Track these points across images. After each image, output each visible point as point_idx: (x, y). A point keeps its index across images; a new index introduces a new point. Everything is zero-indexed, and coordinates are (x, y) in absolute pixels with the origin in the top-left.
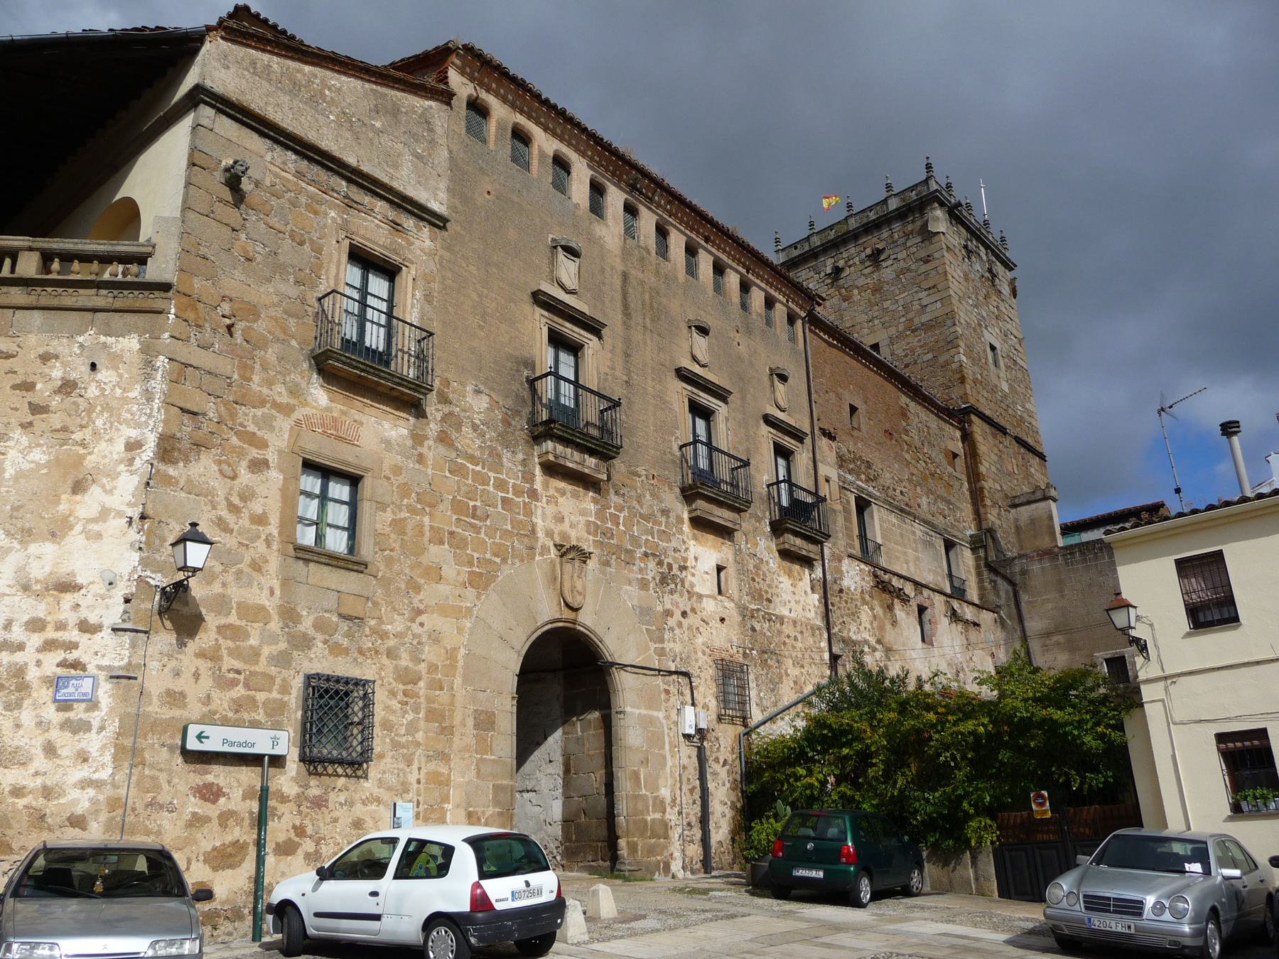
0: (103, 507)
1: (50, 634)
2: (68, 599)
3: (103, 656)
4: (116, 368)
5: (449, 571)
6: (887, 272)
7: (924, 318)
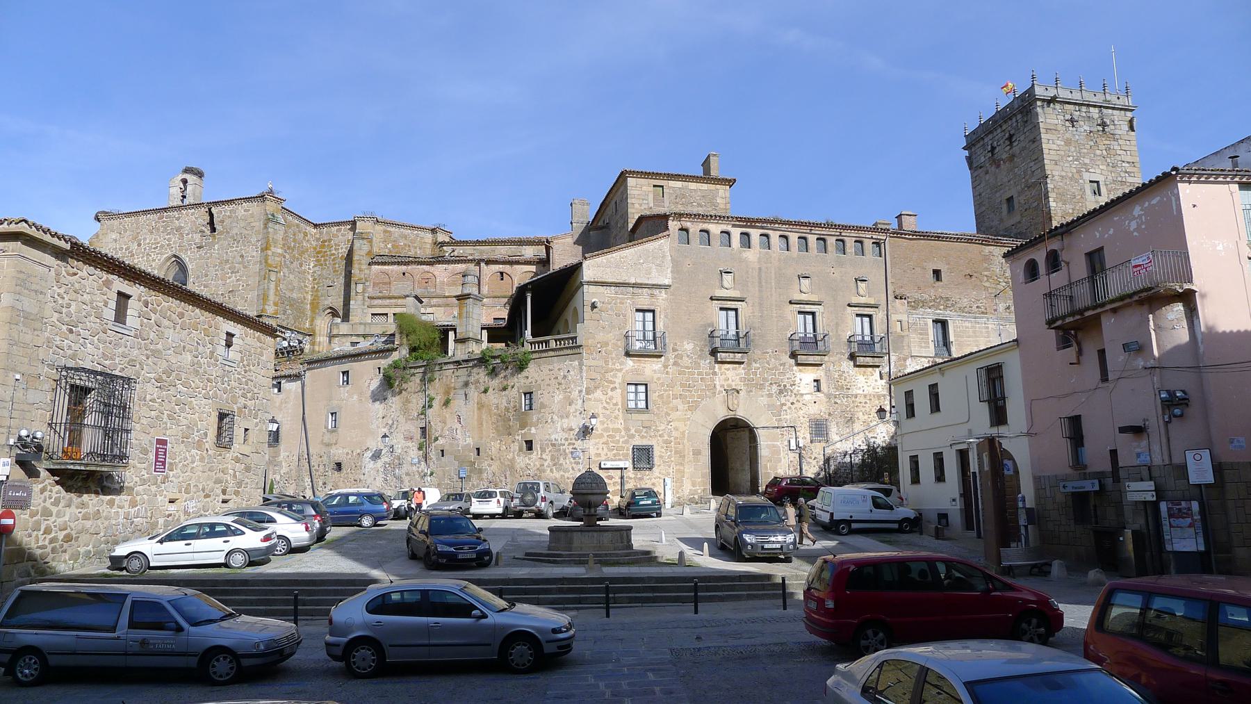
5: (680, 407)
6: (1016, 149)
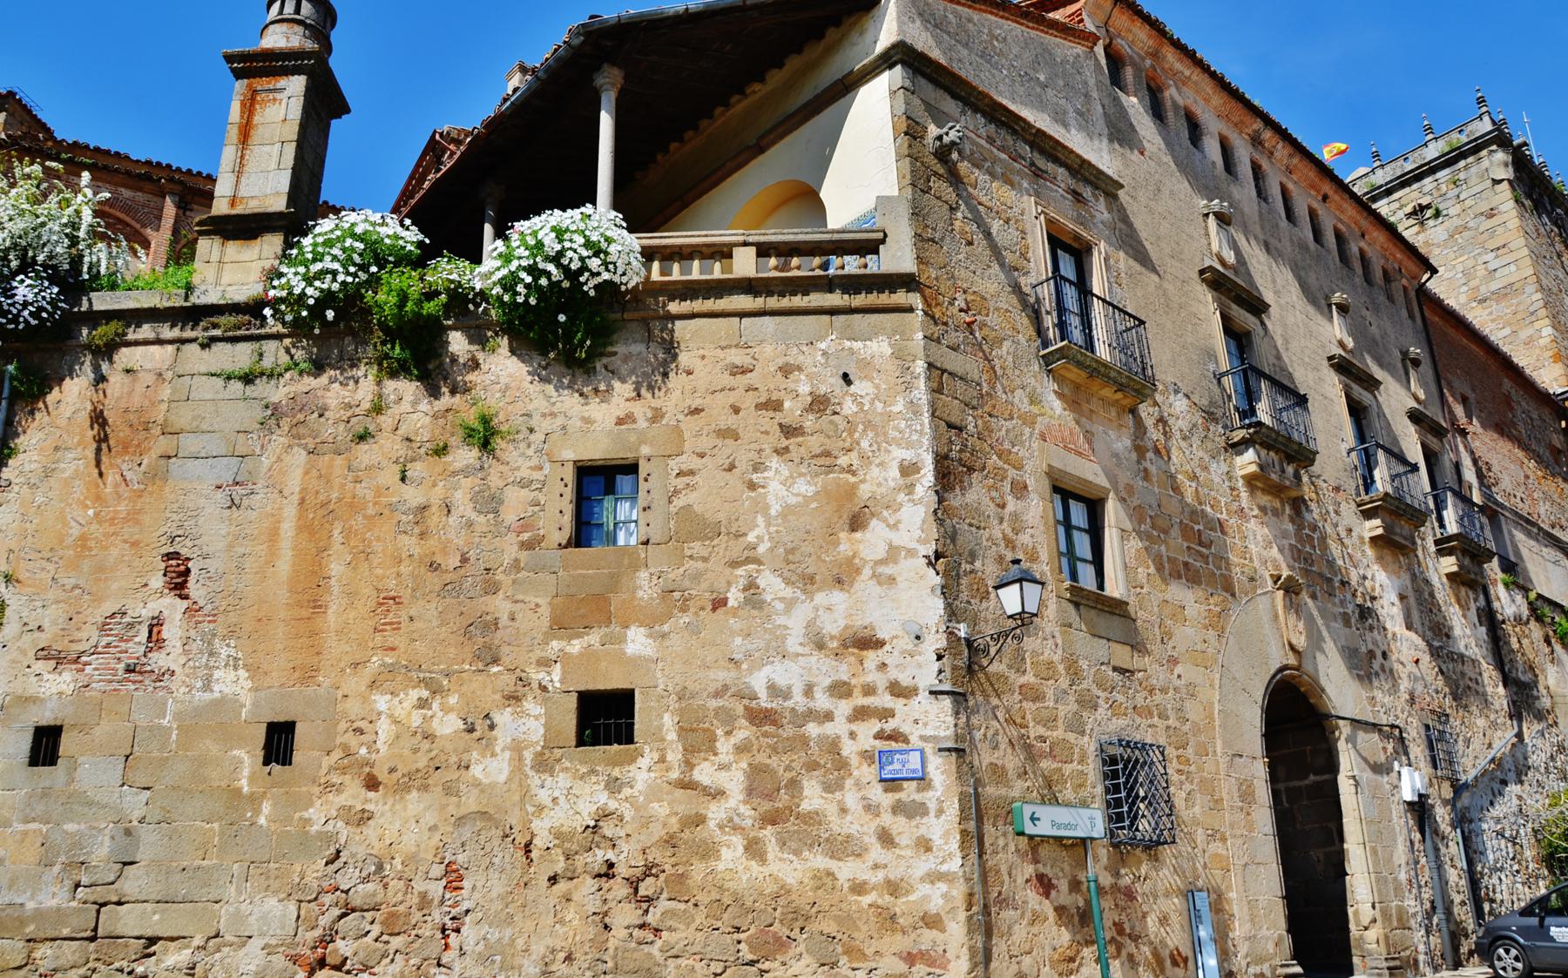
0: (891, 546)
1: (861, 701)
2: (872, 658)
3: (925, 724)
4: (871, 379)
7: (1494, 286)
